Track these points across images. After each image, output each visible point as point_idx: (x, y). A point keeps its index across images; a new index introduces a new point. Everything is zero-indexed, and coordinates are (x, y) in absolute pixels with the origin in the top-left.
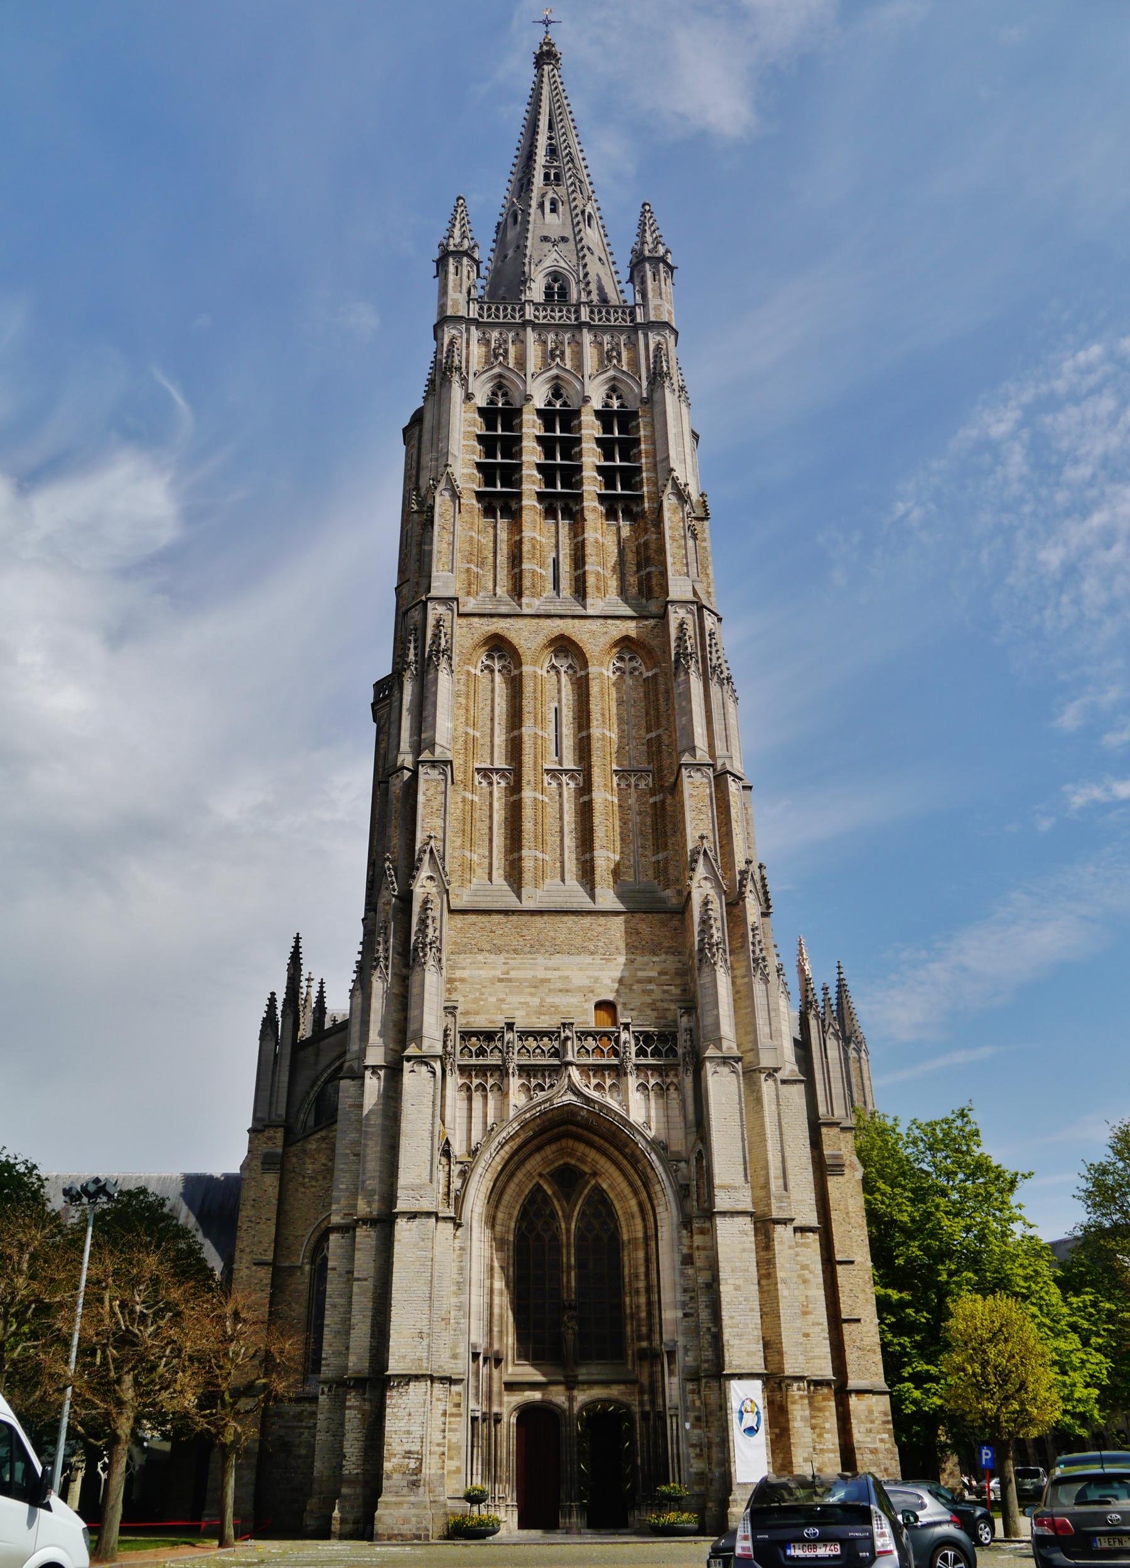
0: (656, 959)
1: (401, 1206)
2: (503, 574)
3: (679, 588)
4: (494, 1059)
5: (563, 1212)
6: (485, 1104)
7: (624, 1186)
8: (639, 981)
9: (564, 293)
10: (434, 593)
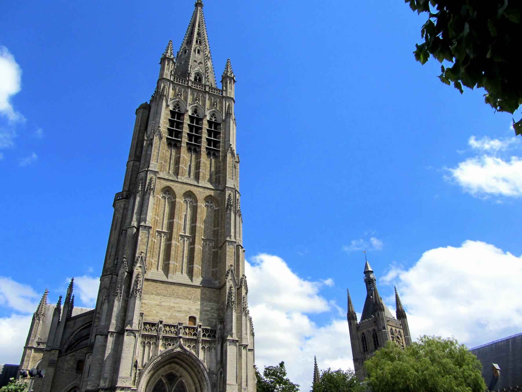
0: (210, 304)
1: (119, 384)
2: (172, 167)
3: (230, 183)
4: (154, 333)
5: (169, 388)
6: (150, 349)
7: (191, 381)
8: (204, 311)
9: (200, 80)
10: (150, 169)
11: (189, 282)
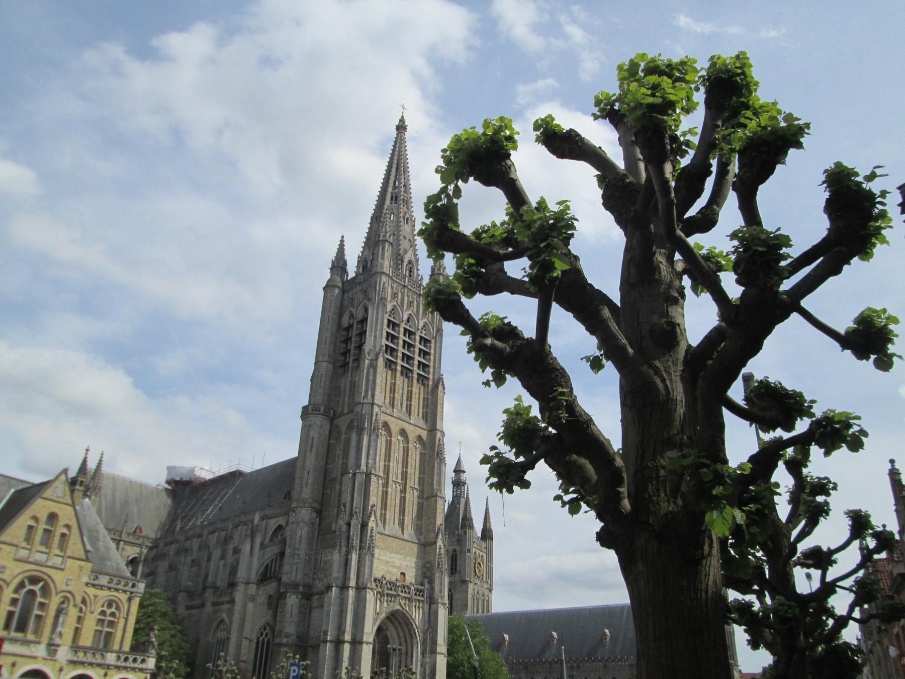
11: (399, 534)
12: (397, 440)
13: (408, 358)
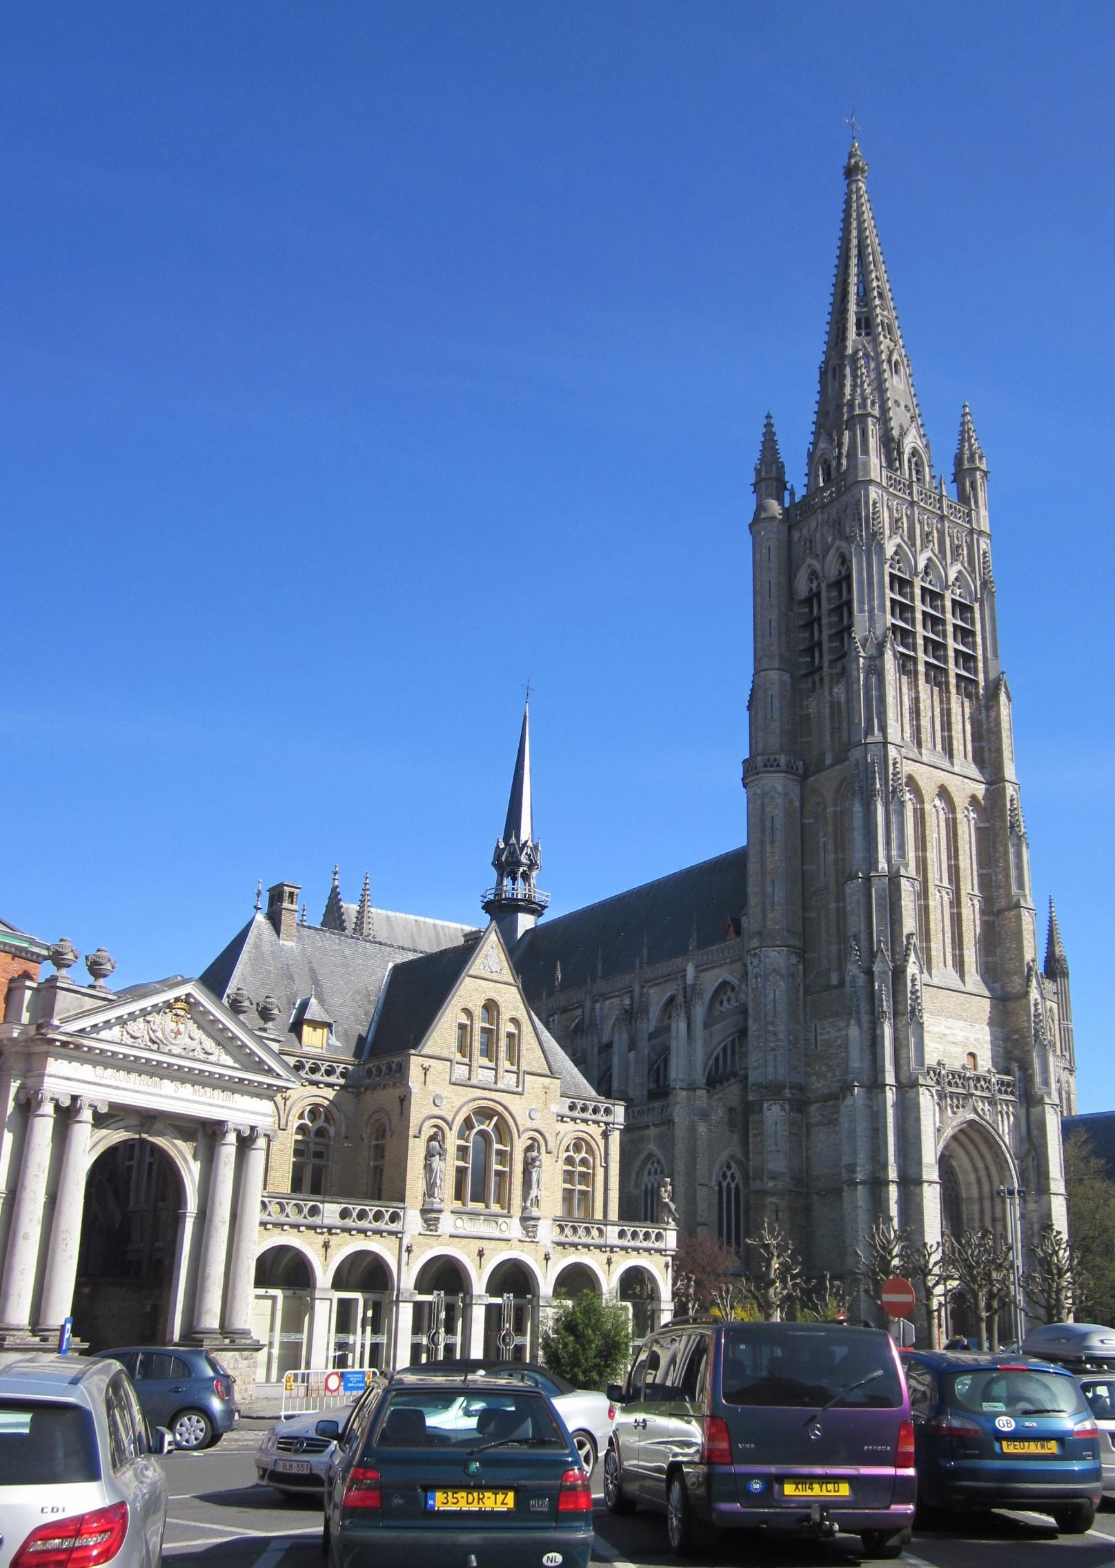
12: (934, 809)
13: (936, 647)
